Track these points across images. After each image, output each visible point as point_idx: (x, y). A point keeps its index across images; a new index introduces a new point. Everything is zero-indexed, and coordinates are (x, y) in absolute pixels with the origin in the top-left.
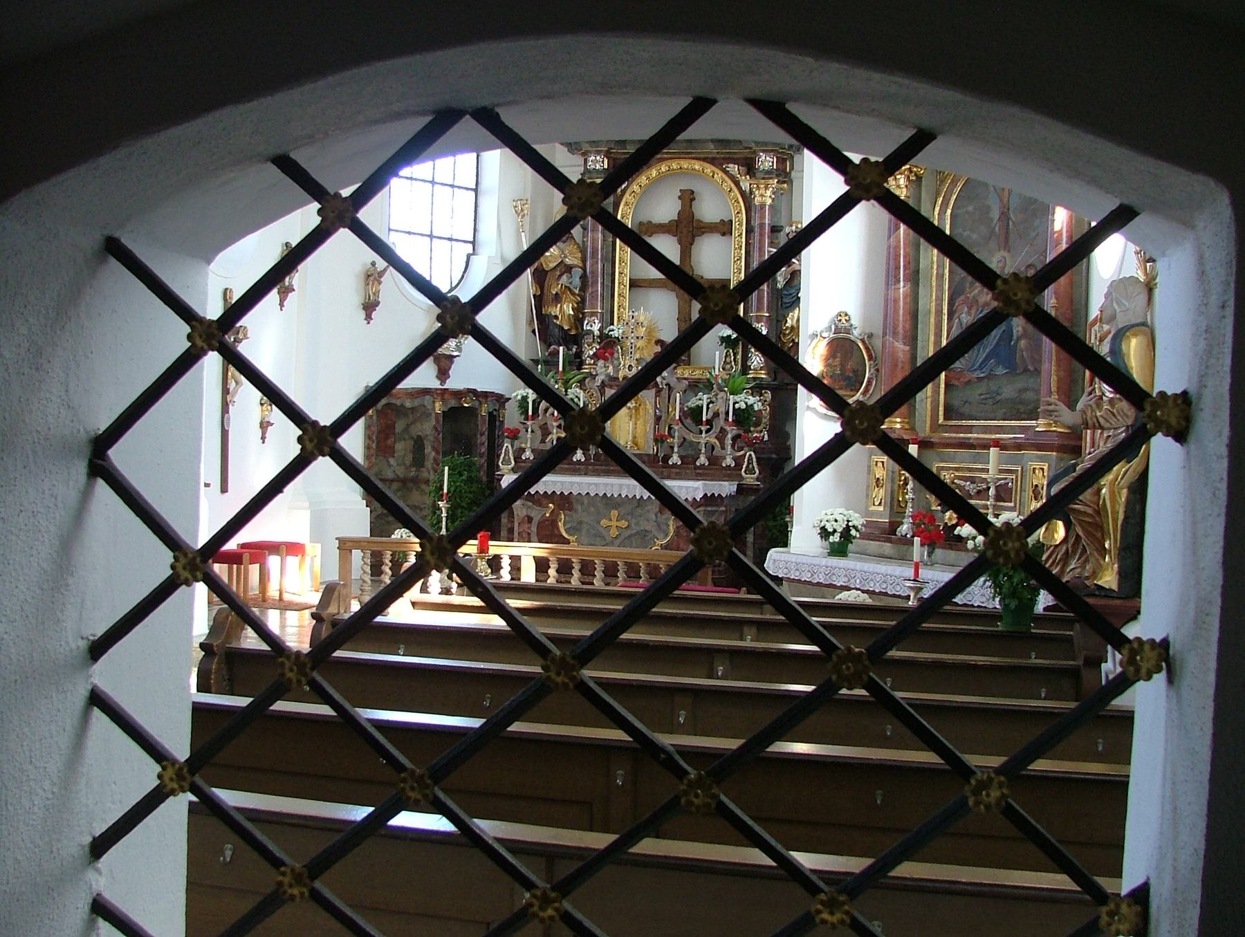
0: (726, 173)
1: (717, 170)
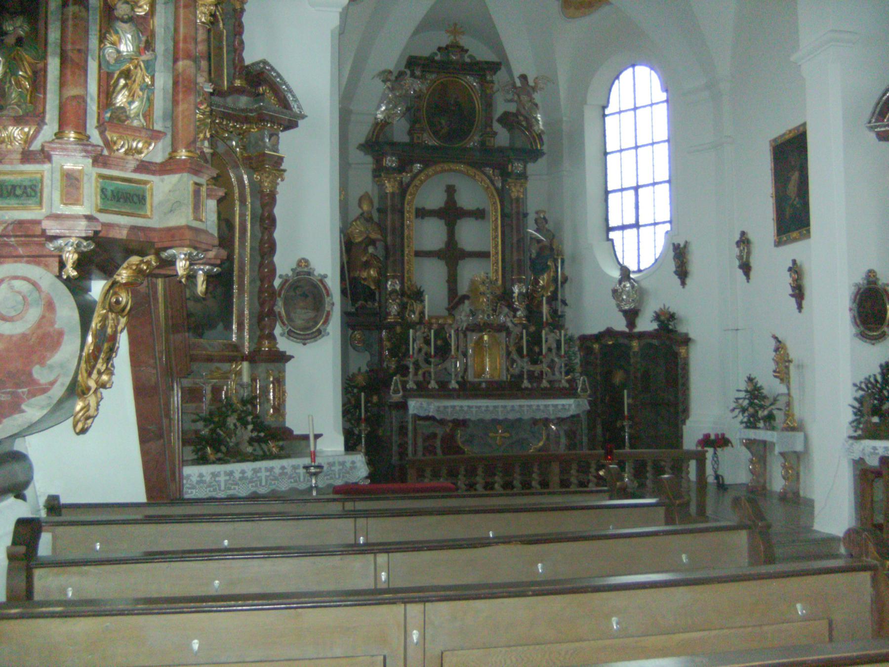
0: (485, 174)
1: (477, 172)
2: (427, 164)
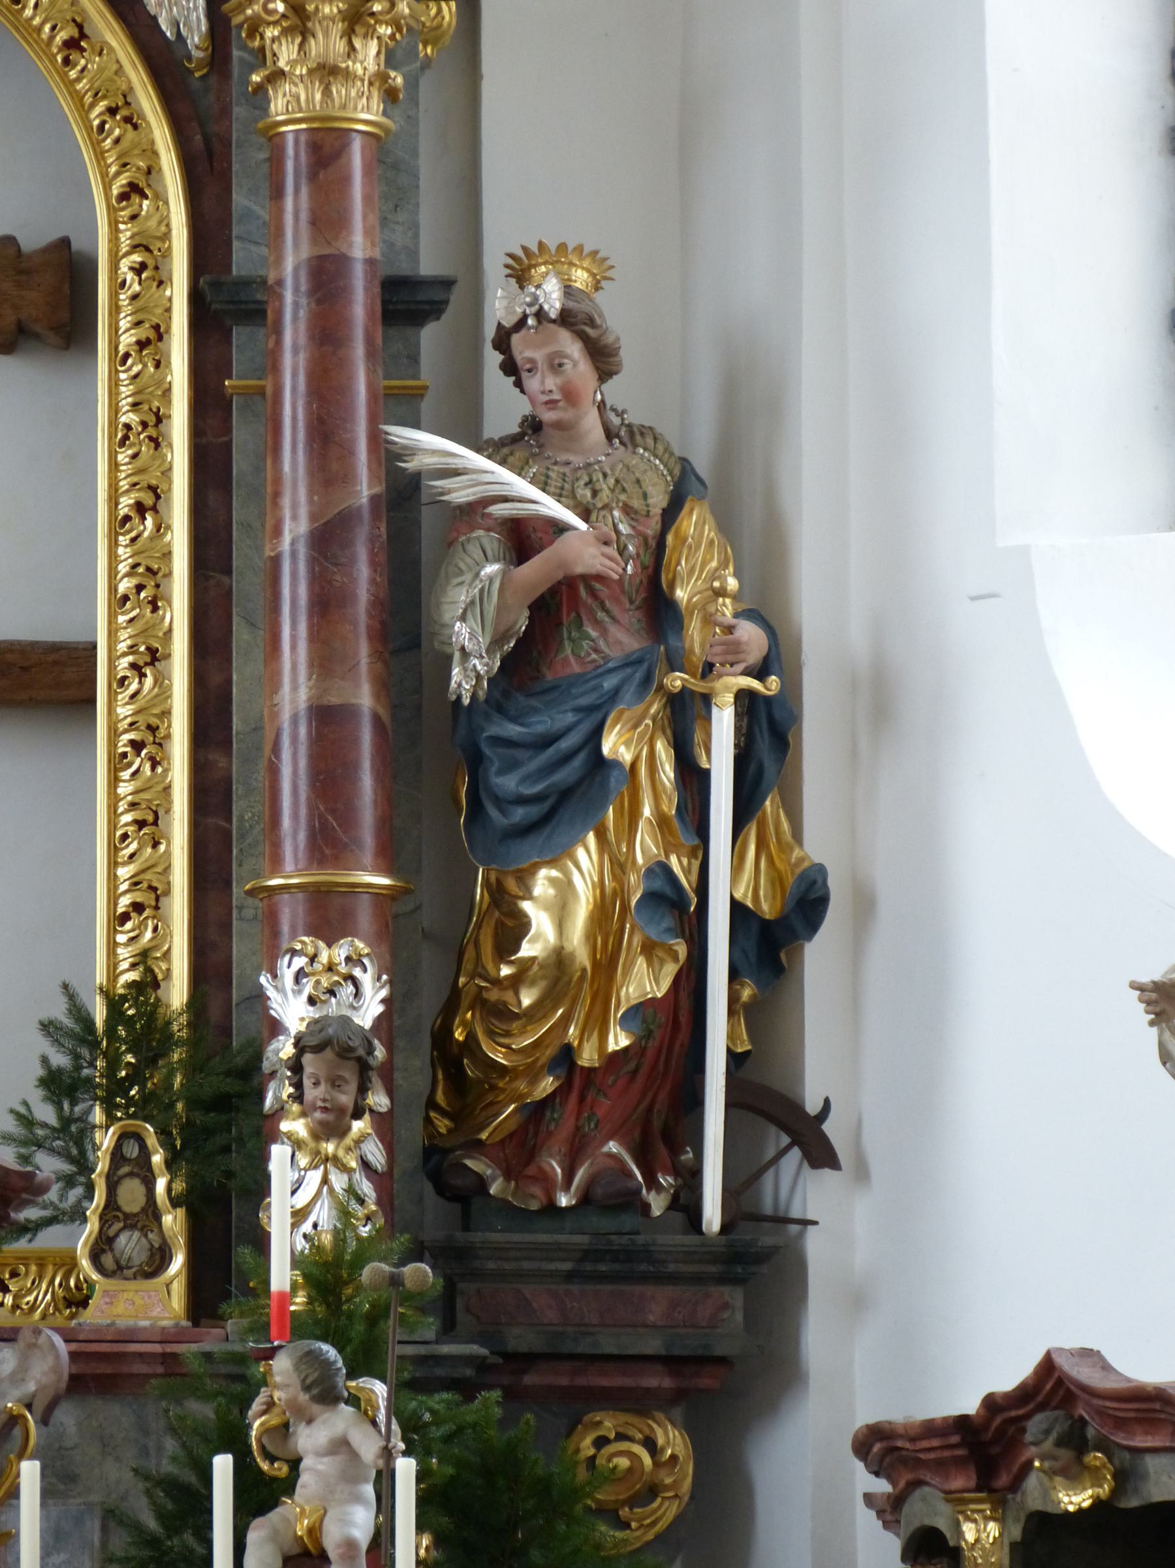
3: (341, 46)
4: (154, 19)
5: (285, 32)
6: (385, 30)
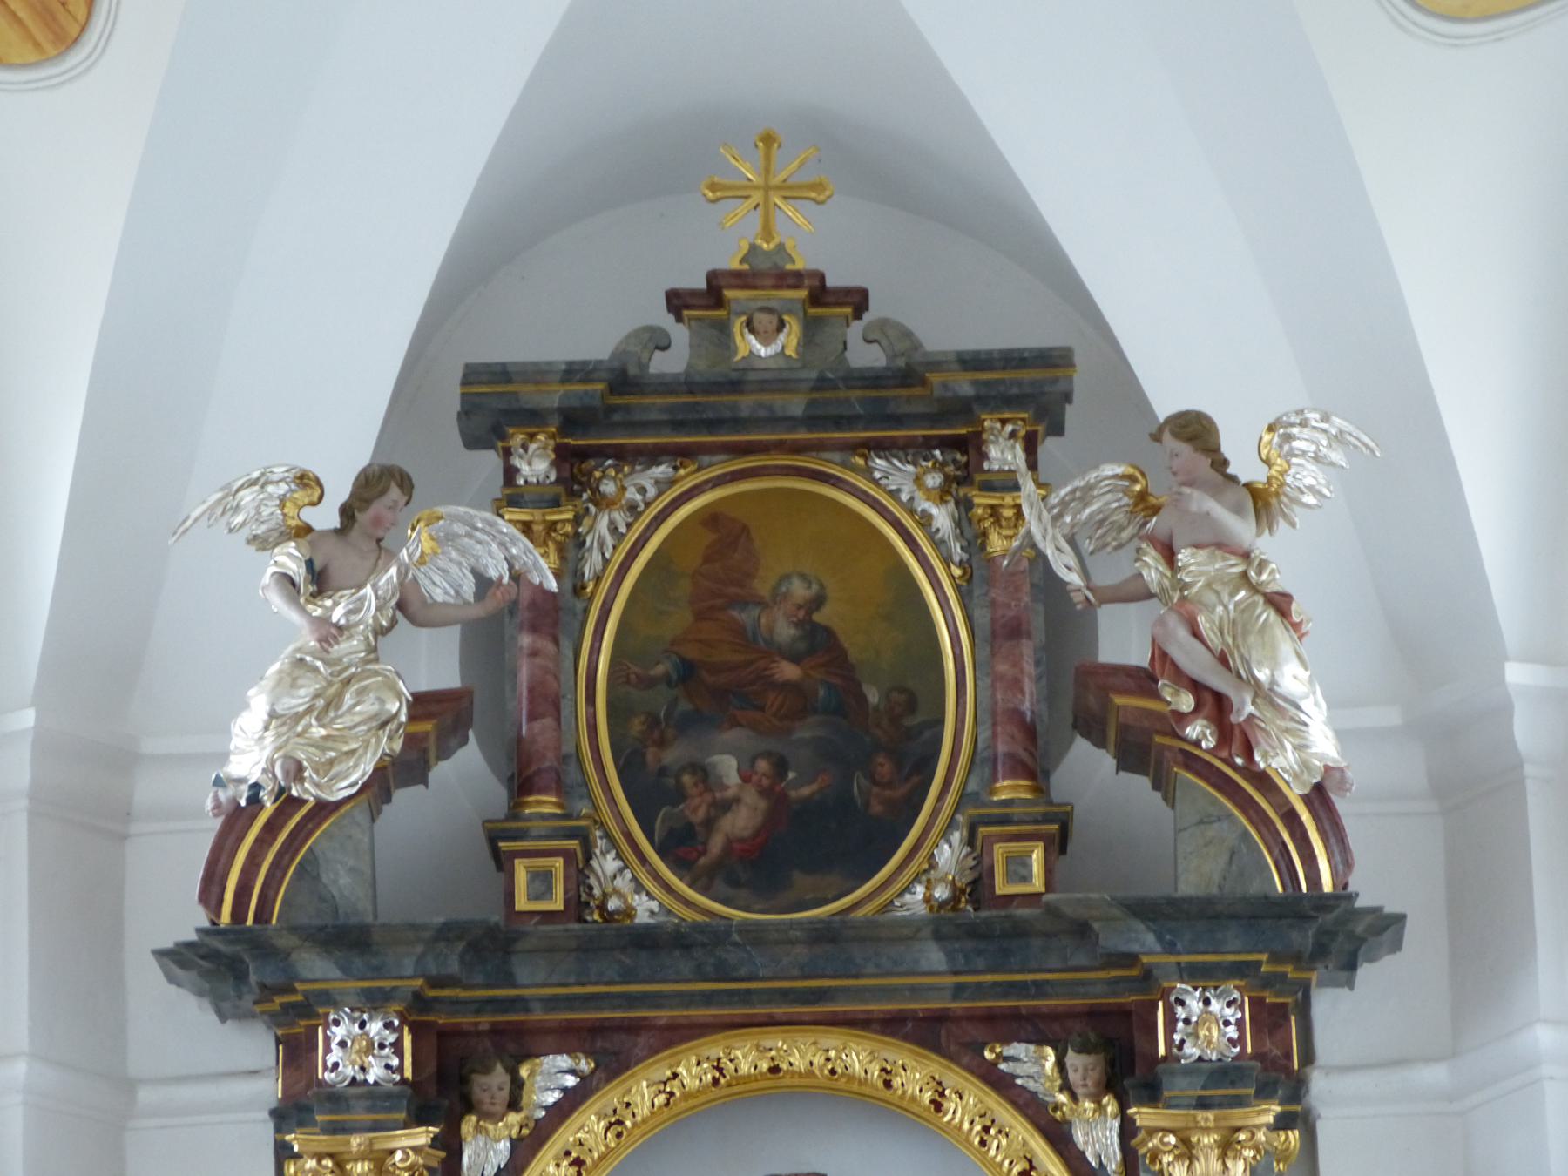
0: (1001, 1083)
1: (954, 1078)
2: (612, 1049)
3: (1218, 1166)
4: (1083, 1153)
5: (1177, 1158)
6: (1248, 1153)
